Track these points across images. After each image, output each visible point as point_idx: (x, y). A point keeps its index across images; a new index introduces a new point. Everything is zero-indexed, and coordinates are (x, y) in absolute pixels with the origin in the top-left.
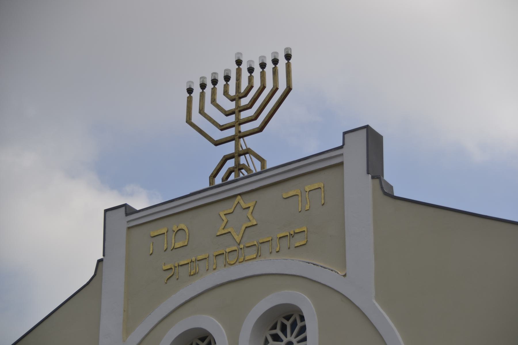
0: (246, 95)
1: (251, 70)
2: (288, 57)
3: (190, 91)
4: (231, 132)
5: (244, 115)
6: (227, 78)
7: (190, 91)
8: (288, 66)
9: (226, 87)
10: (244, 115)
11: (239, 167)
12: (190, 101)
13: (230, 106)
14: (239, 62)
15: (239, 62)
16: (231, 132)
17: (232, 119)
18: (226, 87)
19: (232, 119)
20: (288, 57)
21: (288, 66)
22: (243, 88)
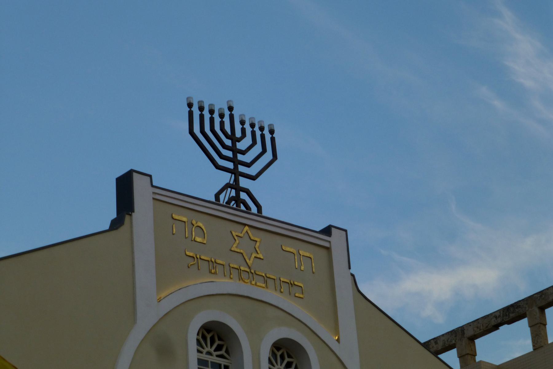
0: (239, 140)
1: (242, 123)
2: (272, 132)
3: (190, 105)
4: (230, 165)
5: (240, 157)
6: (222, 116)
7: (190, 105)
8: (273, 140)
9: (222, 124)
10: (240, 157)
11: (237, 200)
12: (191, 114)
13: (228, 142)
14: (231, 109)
15: (231, 109)
16: (230, 165)
17: (229, 154)
18: (222, 124)
19: (229, 154)
20: (272, 132)
21: (273, 140)
22: (238, 134)
